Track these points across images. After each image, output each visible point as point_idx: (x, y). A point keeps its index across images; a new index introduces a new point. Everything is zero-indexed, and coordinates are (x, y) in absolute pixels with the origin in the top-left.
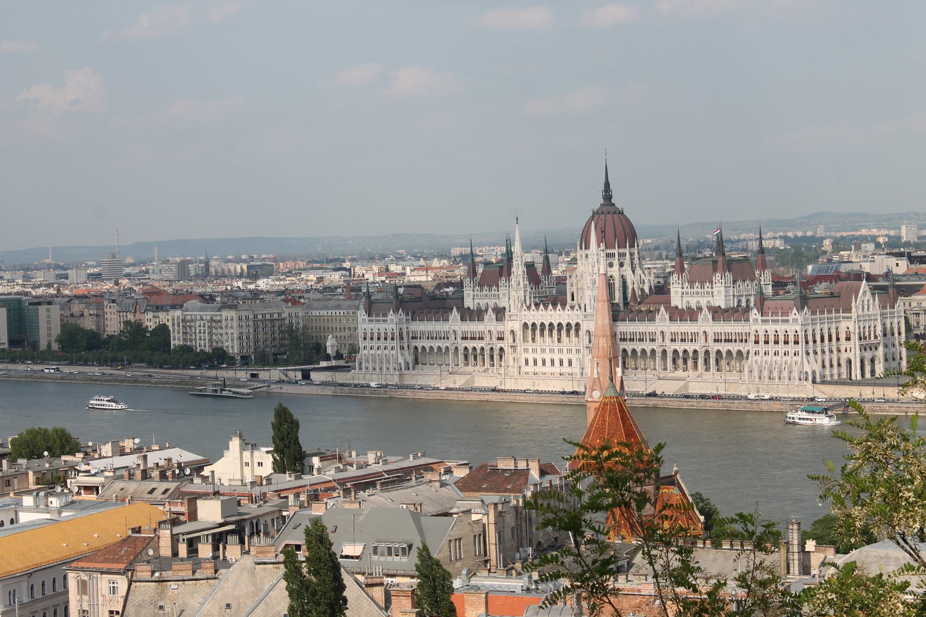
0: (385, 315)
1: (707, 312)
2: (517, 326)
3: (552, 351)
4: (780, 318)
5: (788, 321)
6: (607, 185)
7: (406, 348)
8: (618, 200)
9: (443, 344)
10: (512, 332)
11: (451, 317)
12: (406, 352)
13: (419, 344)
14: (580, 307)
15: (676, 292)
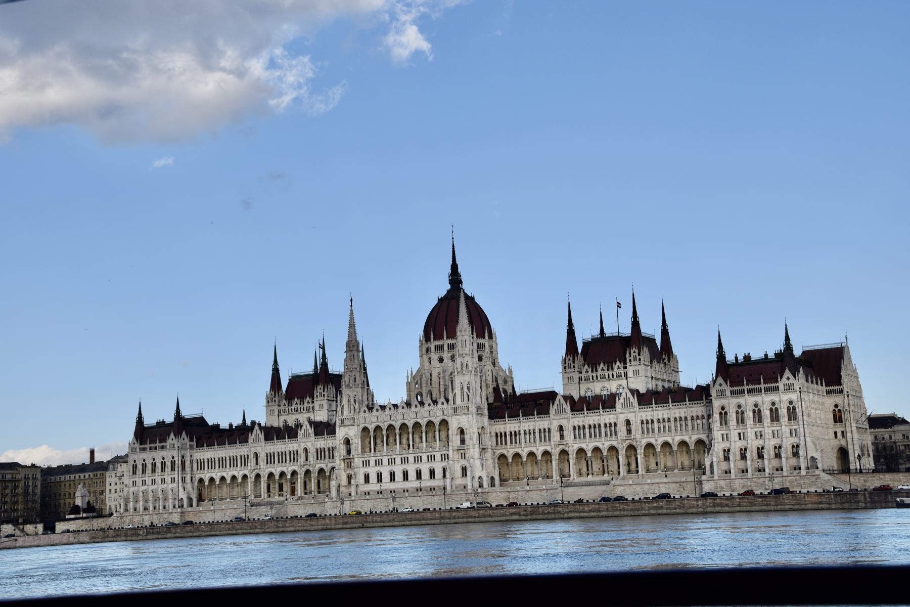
0: (164, 440)
1: (629, 395)
2: (353, 433)
3: (405, 461)
4: (763, 386)
5: (777, 389)
6: (454, 267)
7: (188, 479)
8: (468, 287)
9: (239, 473)
10: (348, 442)
11: (251, 438)
12: (189, 486)
13: (206, 475)
14: (447, 400)
15: (571, 379)
